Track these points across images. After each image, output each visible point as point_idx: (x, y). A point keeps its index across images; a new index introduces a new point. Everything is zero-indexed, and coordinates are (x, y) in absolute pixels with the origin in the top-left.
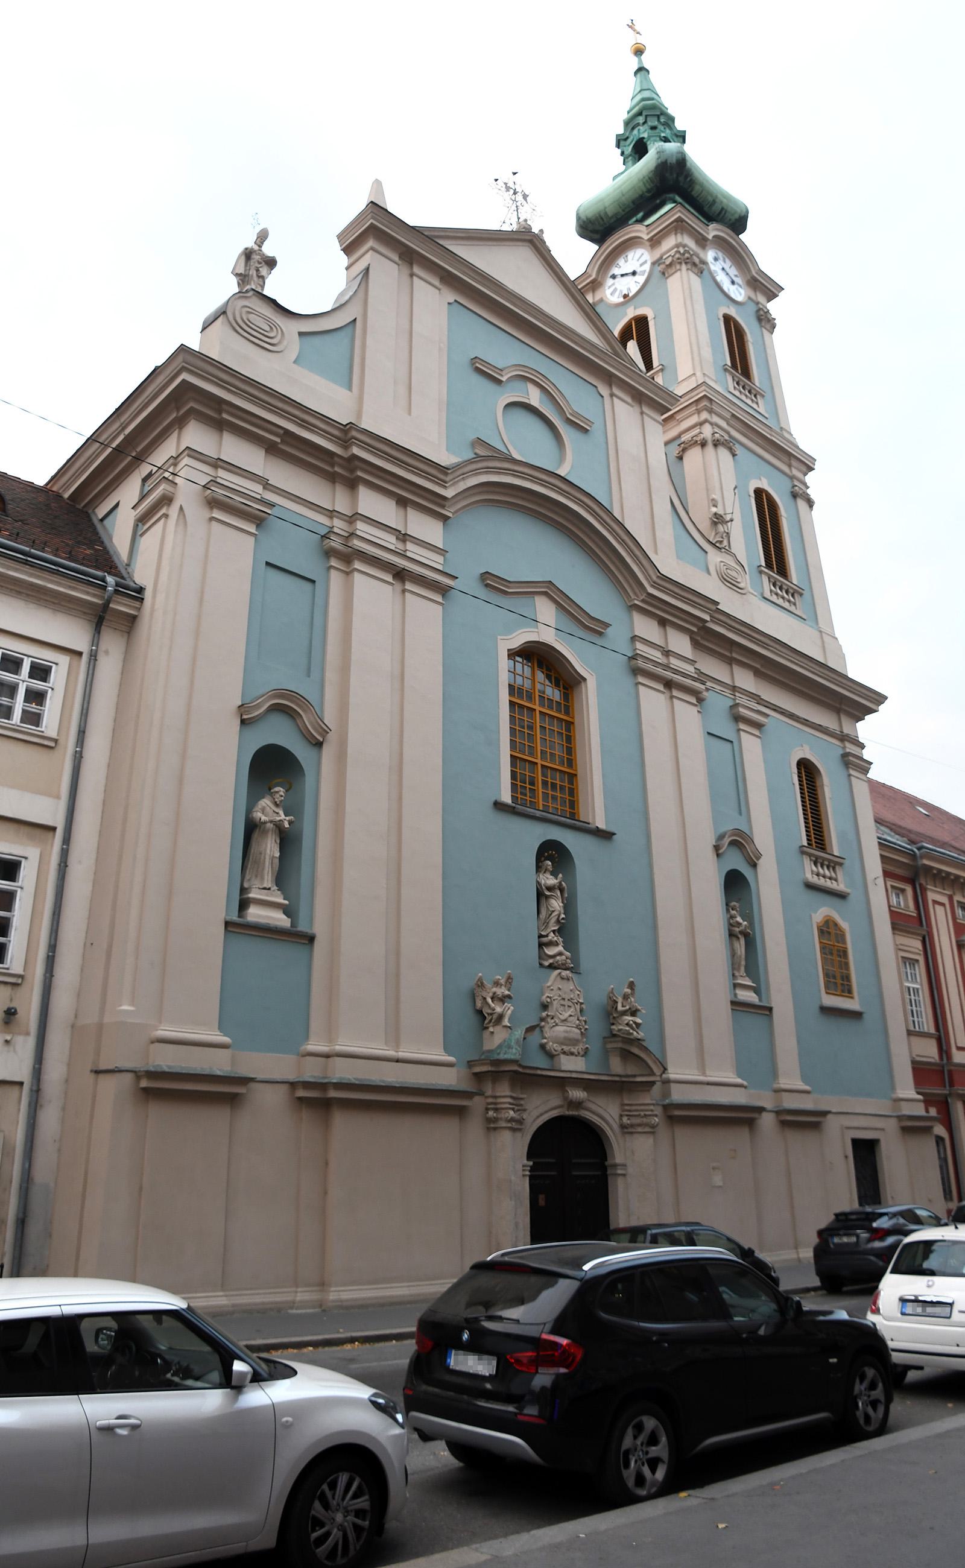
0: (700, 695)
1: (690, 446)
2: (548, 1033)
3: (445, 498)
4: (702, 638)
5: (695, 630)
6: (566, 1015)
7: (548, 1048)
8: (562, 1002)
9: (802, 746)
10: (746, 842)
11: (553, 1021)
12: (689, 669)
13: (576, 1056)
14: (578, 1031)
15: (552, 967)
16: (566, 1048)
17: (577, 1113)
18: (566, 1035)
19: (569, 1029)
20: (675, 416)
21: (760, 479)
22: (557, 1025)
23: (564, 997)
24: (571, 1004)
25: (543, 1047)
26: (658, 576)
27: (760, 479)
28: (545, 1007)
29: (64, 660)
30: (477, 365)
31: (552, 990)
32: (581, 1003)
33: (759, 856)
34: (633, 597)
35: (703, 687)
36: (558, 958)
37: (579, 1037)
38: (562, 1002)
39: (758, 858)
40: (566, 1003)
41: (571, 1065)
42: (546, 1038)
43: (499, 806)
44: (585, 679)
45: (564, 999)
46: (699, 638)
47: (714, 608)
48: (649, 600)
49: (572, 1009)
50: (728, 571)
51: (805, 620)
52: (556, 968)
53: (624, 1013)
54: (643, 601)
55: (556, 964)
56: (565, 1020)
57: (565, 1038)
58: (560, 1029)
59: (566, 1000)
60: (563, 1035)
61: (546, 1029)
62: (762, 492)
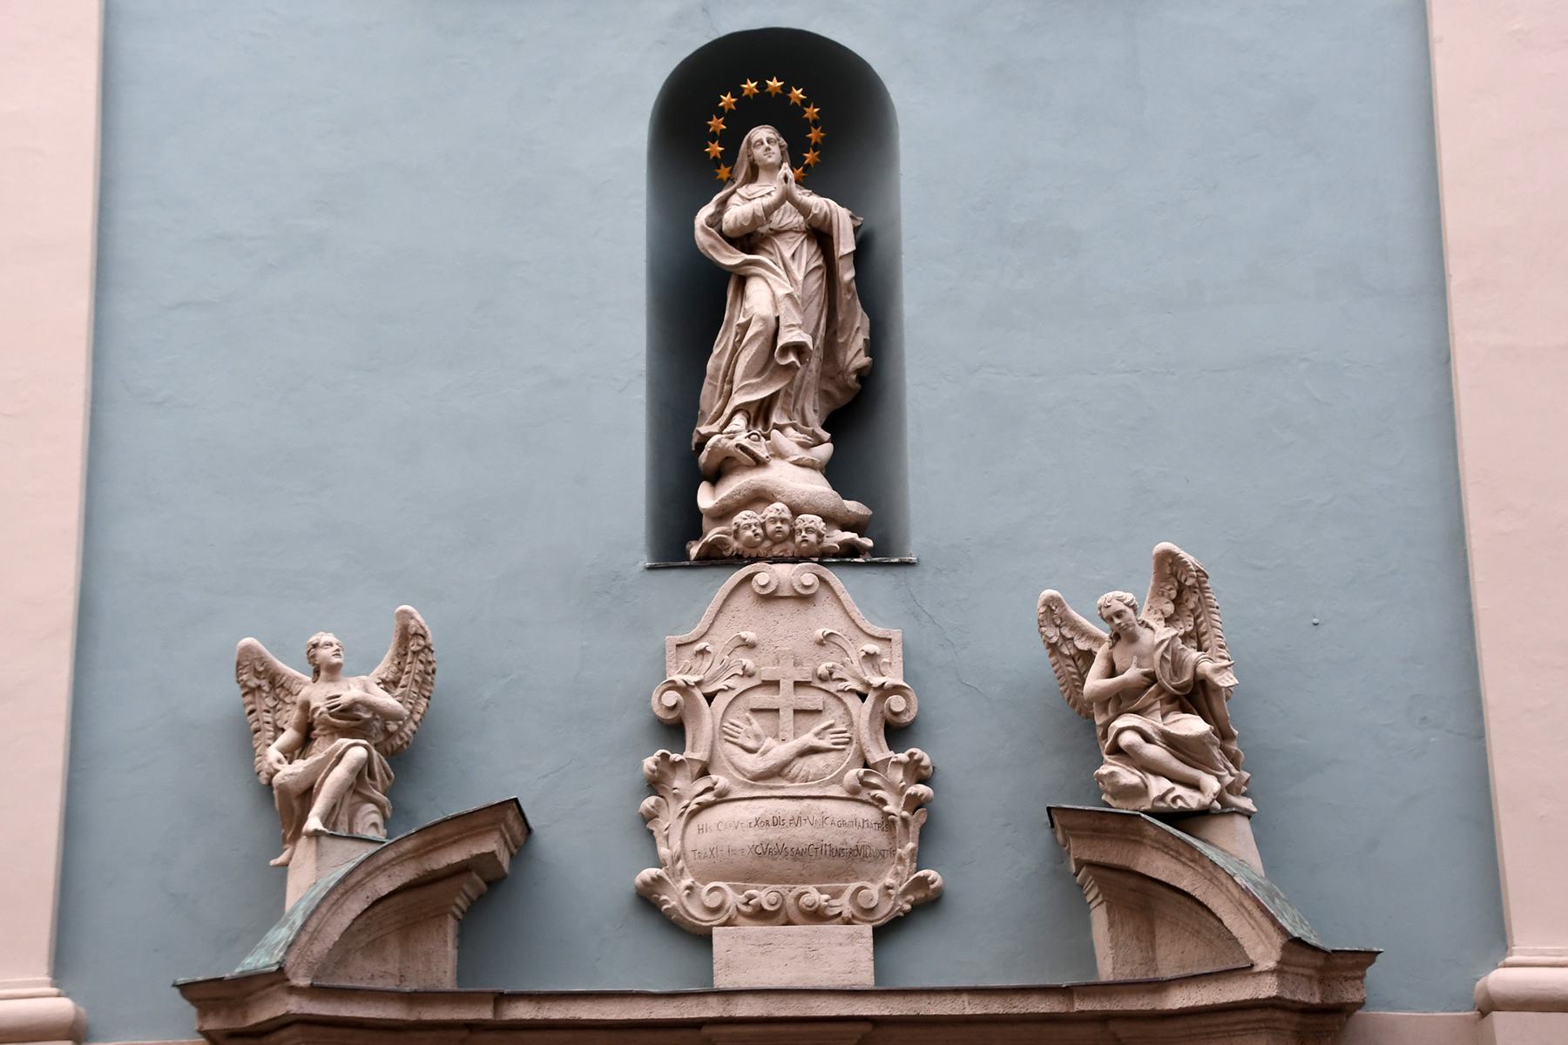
2: (672, 834)
6: (779, 751)
7: (672, 899)
8: (762, 698)
13: (848, 922)
14: (868, 814)
15: (716, 558)
16: (765, 895)
18: (772, 835)
22: (723, 798)
23: (767, 673)
24: (811, 699)
25: (648, 900)
28: (674, 730)
31: (703, 652)
32: (885, 691)
40: (785, 698)
45: (773, 684)
52: (739, 560)
53: (1123, 699)
55: (736, 545)
57: (767, 851)
59: (787, 685)
60: (752, 837)
61: (670, 820)
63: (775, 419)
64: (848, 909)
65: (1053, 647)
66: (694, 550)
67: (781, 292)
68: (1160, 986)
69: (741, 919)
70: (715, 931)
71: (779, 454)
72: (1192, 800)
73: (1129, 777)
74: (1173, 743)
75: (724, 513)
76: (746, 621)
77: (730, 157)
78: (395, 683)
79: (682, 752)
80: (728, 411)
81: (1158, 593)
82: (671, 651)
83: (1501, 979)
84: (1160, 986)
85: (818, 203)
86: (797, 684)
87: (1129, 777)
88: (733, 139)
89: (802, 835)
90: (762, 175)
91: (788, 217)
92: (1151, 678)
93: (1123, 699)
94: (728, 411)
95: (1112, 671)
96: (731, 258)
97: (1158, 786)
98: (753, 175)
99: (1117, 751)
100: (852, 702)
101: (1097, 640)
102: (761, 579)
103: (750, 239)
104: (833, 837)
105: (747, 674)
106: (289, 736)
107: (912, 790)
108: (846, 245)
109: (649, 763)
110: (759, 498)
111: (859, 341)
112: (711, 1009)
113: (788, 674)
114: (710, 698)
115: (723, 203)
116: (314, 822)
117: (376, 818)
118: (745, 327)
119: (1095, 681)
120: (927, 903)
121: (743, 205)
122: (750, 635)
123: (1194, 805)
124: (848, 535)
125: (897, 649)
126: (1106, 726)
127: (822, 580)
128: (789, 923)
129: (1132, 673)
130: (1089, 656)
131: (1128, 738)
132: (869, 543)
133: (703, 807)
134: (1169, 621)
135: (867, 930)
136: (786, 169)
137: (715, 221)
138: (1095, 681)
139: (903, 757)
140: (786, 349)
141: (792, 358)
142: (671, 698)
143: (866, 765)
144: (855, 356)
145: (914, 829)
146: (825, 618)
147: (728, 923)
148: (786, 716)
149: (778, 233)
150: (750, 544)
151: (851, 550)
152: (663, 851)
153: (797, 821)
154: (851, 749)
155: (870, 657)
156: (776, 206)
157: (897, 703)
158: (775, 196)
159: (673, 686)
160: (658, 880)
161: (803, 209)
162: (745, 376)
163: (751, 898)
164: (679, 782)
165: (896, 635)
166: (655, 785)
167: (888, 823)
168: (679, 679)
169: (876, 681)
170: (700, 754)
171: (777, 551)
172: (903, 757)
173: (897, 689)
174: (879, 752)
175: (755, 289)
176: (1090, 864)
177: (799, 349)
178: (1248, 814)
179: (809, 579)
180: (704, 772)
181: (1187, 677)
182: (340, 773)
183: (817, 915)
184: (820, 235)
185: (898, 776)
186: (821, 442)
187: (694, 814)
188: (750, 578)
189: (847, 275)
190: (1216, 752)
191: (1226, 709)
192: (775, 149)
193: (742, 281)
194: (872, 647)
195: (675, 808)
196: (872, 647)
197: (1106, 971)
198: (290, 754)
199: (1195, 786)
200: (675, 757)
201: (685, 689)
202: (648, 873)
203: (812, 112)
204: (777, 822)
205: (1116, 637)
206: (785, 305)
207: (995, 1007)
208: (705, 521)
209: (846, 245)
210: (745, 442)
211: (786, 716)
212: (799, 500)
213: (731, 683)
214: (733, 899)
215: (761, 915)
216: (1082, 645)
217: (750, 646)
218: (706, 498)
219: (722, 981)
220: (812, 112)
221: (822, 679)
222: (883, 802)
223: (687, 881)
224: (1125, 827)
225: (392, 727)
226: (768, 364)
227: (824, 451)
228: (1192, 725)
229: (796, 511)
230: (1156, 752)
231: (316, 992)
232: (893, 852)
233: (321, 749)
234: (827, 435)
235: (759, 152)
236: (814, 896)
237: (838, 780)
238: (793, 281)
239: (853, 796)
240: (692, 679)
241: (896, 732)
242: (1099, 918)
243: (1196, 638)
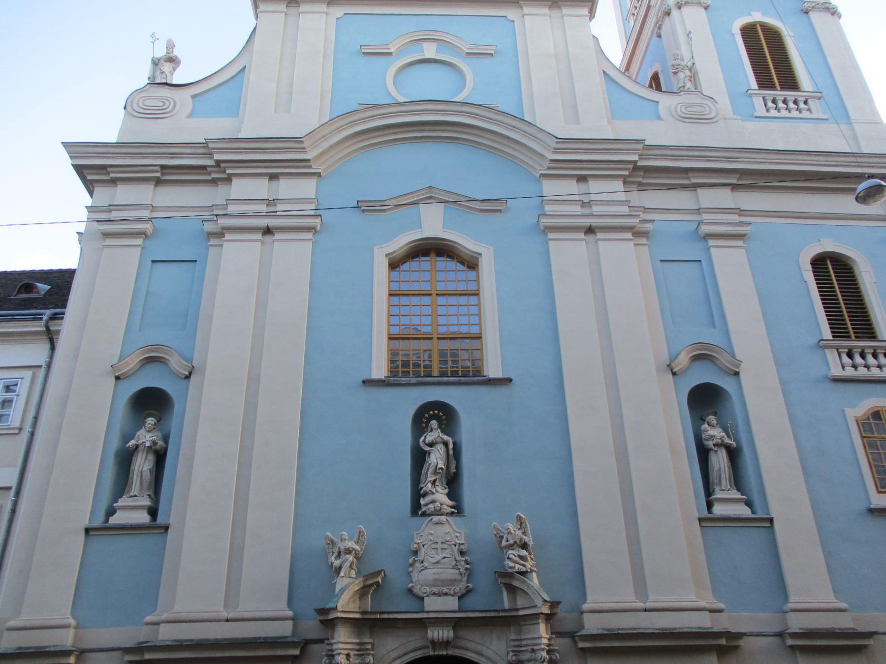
0: (635, 230)
1: (662, 21)
2: (415, 576)
3: (308, 161)
4: (643, 177)
5: (627, 173)
6: (439, 558)
7: (416, 590)
8: (434, 546)
9: (820, 241)
10: (710, 350)
11: (422, 565)
12: (625, 209)
13: (453, 596)
14: (457, 571)
15: (424, 514)
16: (435, 590)
17: (445, 653)
18: (436, 576)
19: (441, 570)
20: (651, 4)
21: (751, 15)
22: (426, 568)
23: (435, 541)
24: (445, 546)
25: (410, 591)
26: (557, 142)
27: (751, 15)
28: (416, 553)
29: (28, 374)
30: (363, 51)
31: (422, 535)
32: (460, 544)
33: (738, 364)
34: (538, 168)
35: (636, 221)
36: (431, 506)
37: (459, 577)
38: (434, 546)
39: (738, 366)
40: (440, 546)
41: (433, 605)
42: (413, 583)
43: (368, 383)
44: (480, 254)
45: (437, 543)
46: (641, 179)
47: (640, 146)
48: (554, 165)
49: (447, 551)
50: (688, 109)
51: (827, 119)
52: (429, 515)
54: (549, 168)
56: (438, 562)
57: (435, 580)
58: (430, 574)
62: (755, 25)
63: (437, 483)
64: (453, 593)
65: (495, 535)
66: (420, 513)
67: (437, 457)
68: (517, 610)
69: (431, 595)
70: (425, 598)
71: (437, 491)
72: (523, 569)
73: (512, 564)
74: (520, 557)
75: (426, 505)
76: (432, 529)
77: (427, 427)
78: (358, 542)
79: (417, 558)
80: (427, 482)
81: (517, 523)
82: (415, 536)
83: (585, 607)
84: (517, 610)
85: (446, 437)
86: (442, 543)
87: (512, 564)
88: (428, 423)
89: (443, 577)
90: (433, 430)
91: (439, 440)
92: (515, 542)
93: (511, 547)
94: (427, 482)
95: (507, 541)
96: (427, 449)
97: (517, 566)
98: (432, 430)
99: (508, 558)
100: (453, 546)
101: (504, 533)
102: (434, 520)
103: (431, 445)
104: (450, 577)
105: (431, 540)
106: (336, 554)
107: (466, 566)
108: (451, 446)
109: (411, 560)
110: (433, 502)
111: (454, 467)
112: (424, 615)
113: (440, 540)
114: (423, 546)
115: (426, 437)
116: (342, 574)
117: (354, 573)
118: (430, 464)
119: (504, 543)
120: (469, 591)
121: (430, 437)
122: (432, 532)
123: (525, 571)
124: (453, 510)
125: (463, 536)
126: (507, 552)
127: (447, 520)
128: (440, 596)
129: (511, 542)
130: (502, 537)
131: (511, 556)
132: (456, 511)
133: (422, 570)
134: (519, 529)
135: (457, 598)
136: (439, 430)
137: (424, 441)
138: (504, 543)
139: (464, 559)
140: (439, 469)
141: (440, 471)
142: (415, 546)
143: (456, 561)
144: (453, 470)
145: (466, 575)
146: (447, 528)
147: (427, 596)
148: (439, 550)
149: (437, 443)
150: (432, 512)
151: (453, 513)
152: (414, 580)
153: (442, 573)
154: (453, 558)
155: (457, 536)
156: (437, 438)
157: (462, 547)
158: (436, 436)
159: (416, 543)
160: (413, 586)
161: (443, 439)
162: (430, 474)
163: (432, 590)
164: (417, 564)
165: (463, 532)
166: (412, 565)
167: (461, 574)
168: (417, 541)
169: (458, 542)
170: (422, 558)
171: (437, 513)
172: (464, 559)
173: (463, 544)
174: (459, 558)
175: (432, 455)
176: (503, 583)
177: (442, 469)
178: (535, 571)
179: (444, 520)
180: (422, 562)
181: (523, 542)
182: (347, 564)
183: (446, 594)
184: (446, 444)
185: (463, 563)
186: (446, 488)
187: (420, 571)
188: (432, 519)
189: (451, 452)
190: (529, 558)
191: (530, 549)
192: (436, 425)
193: (429, 454)
194: (458, 535)
195: (416, 570)
196: (458, 535)
197: (507, 605)
198: (336, 558)
199: (524, 566)
200: (416, 559)
201: (418, 544)
202: (411, 585)
203: (444, 417)
204: (438, 574)
205: (508, 533)
206: (439, 460)
207: (484, 615)
208: (422, 507)
209: (451, 446)
210: (430, 489)
211: (439, 550)
212: (442, 502)
213: (427, 542)
214: (429, 590)
215: (434, 594)
216: (501, 534)
217: (431, 534)
218: (422, 502)
219: (426, 609)
220: (444, 417)
221: (447, 541)
222: (460, 569)
223: (419, 586)
224: (510, 575)
225: (357, 552)
226: (435, 473)
227: (447, 491)
228: (524, 553)
229: (441, 505)
230: (517, 559)
231: (343, 612)
232: (462, 580)
233: (343, 557)
234: (447, 487)
235: (433, 426)
236: (445, 590)
237: (450, 564)
238: (440, 454)
239: (453, 568)
240: (419, 541)
241: (462, 553)
242: (505, 594)
243: (524, 533)
